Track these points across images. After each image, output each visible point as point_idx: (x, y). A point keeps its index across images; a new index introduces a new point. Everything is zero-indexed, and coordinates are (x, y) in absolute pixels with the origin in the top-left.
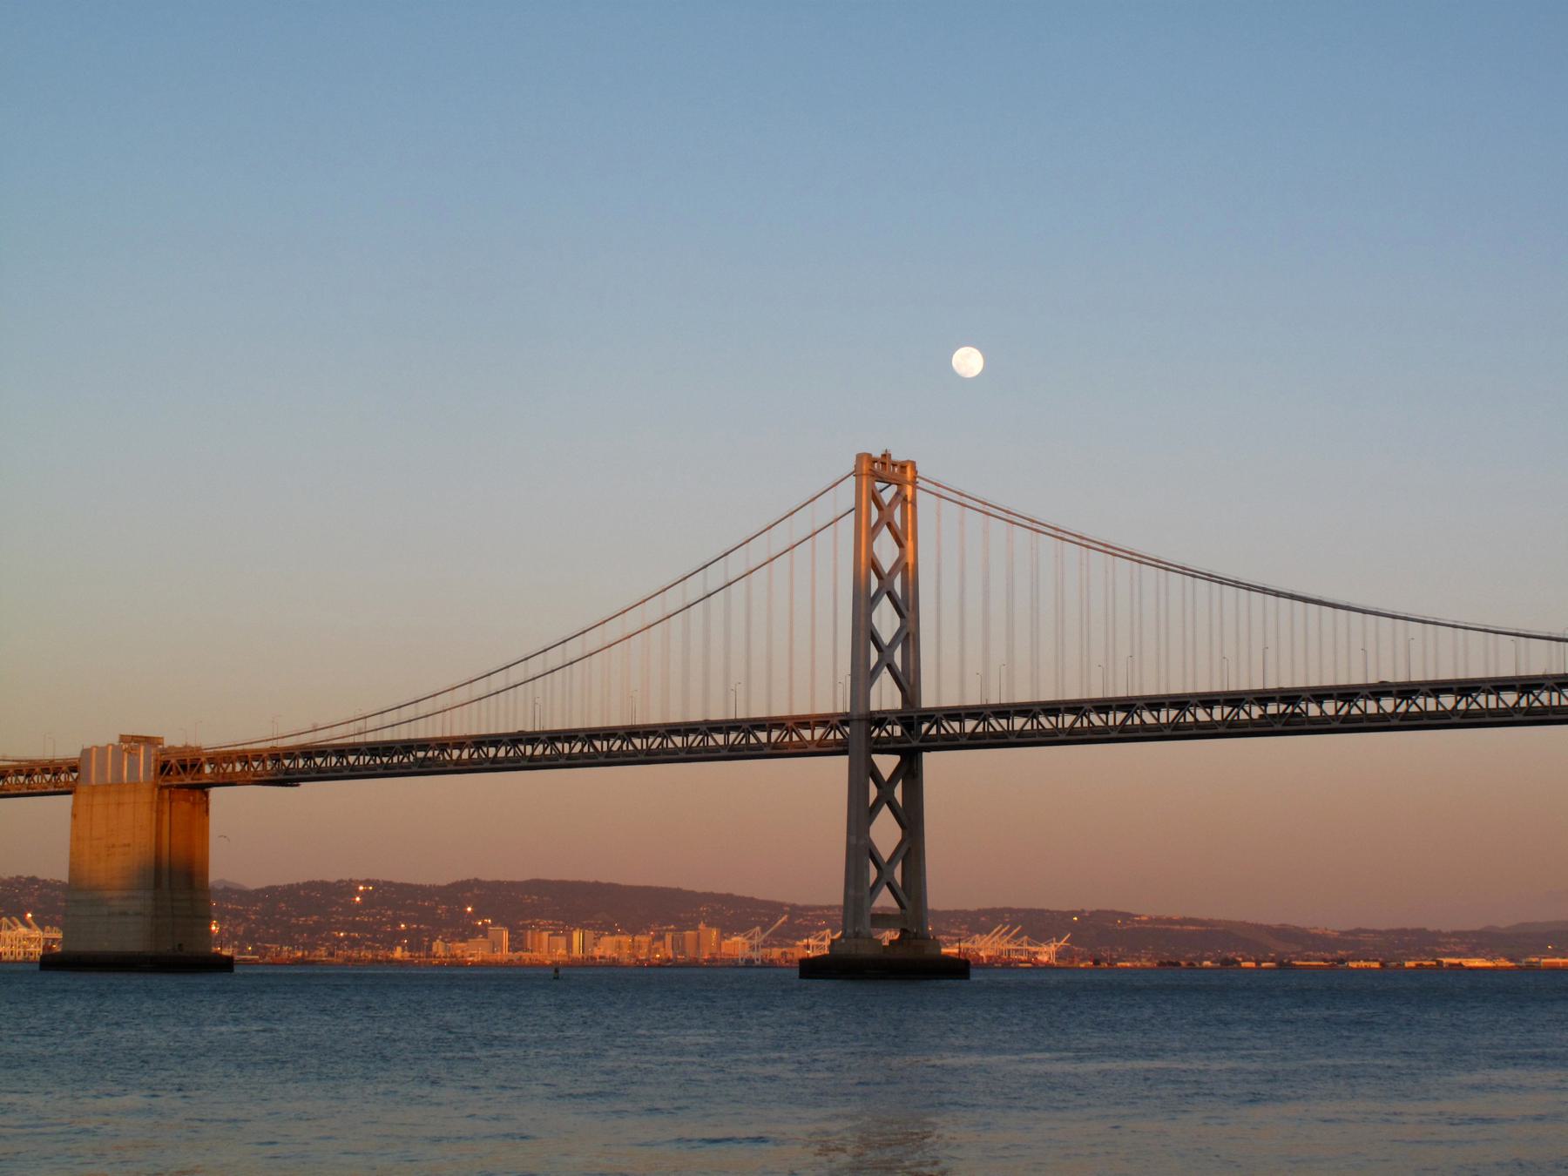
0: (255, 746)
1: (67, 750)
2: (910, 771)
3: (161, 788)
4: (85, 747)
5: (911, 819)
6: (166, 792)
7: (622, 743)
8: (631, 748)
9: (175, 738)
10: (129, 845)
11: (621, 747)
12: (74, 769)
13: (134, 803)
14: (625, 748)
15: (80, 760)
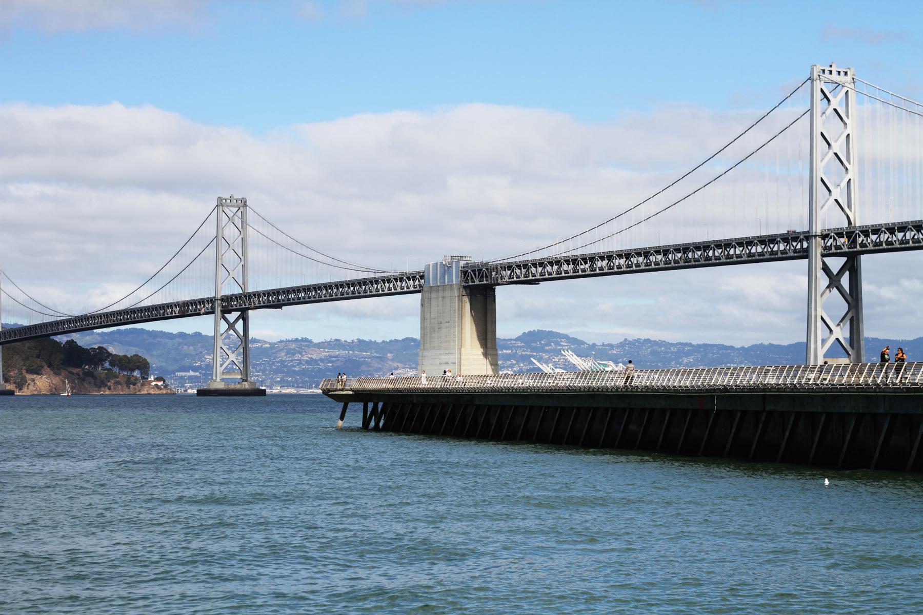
2: (853, 267)
5: (854, 298)
9: (477, 258)
12: (422, 277)
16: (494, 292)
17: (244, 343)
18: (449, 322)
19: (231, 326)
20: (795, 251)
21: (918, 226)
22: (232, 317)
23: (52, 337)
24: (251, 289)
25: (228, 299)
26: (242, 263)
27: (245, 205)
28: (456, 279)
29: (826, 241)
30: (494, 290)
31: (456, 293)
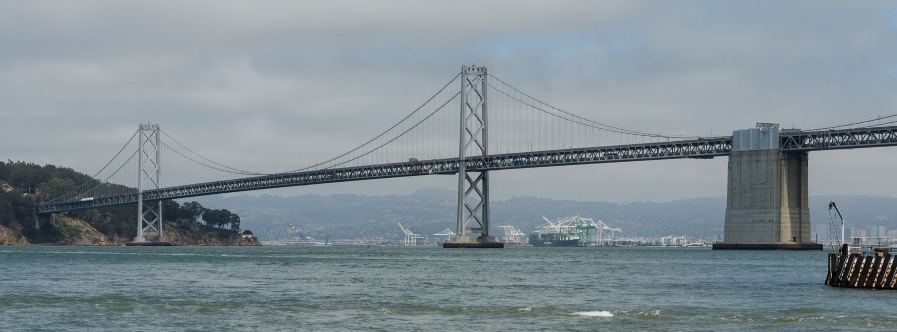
0: (841, 128)
1: (727, 132)
3: (784, 152)
4: (735, 130)
6: (786, 154)
7: (869, 136)
8: (873, 139)
10: (764, 184)
11: (868, 138)
13: (767, 160)
14: (870, 139)
15: (732, 137)
16: (807, 156)
17: (484, 201)
18: (764, 184)
19: (473, 185)
20: (654, 155)
21: (895, 130)
22: (474, 175)
23: (173, 200)
24: (492, 151)
25: (476, 159)
26: (483, 127)
27: (486, 74)
28: (773, 144)
29: (843, 137)
30: (807, 155)
31: (774, 157)
